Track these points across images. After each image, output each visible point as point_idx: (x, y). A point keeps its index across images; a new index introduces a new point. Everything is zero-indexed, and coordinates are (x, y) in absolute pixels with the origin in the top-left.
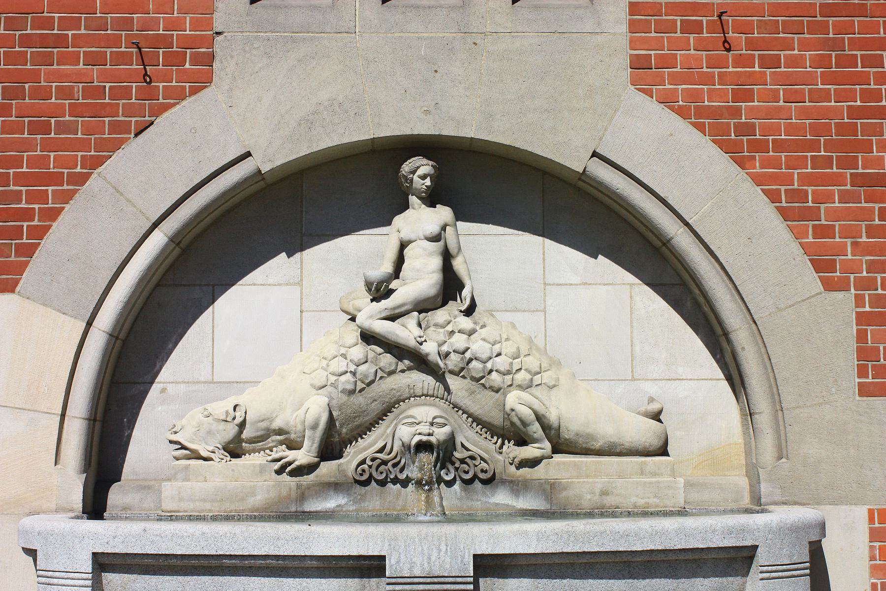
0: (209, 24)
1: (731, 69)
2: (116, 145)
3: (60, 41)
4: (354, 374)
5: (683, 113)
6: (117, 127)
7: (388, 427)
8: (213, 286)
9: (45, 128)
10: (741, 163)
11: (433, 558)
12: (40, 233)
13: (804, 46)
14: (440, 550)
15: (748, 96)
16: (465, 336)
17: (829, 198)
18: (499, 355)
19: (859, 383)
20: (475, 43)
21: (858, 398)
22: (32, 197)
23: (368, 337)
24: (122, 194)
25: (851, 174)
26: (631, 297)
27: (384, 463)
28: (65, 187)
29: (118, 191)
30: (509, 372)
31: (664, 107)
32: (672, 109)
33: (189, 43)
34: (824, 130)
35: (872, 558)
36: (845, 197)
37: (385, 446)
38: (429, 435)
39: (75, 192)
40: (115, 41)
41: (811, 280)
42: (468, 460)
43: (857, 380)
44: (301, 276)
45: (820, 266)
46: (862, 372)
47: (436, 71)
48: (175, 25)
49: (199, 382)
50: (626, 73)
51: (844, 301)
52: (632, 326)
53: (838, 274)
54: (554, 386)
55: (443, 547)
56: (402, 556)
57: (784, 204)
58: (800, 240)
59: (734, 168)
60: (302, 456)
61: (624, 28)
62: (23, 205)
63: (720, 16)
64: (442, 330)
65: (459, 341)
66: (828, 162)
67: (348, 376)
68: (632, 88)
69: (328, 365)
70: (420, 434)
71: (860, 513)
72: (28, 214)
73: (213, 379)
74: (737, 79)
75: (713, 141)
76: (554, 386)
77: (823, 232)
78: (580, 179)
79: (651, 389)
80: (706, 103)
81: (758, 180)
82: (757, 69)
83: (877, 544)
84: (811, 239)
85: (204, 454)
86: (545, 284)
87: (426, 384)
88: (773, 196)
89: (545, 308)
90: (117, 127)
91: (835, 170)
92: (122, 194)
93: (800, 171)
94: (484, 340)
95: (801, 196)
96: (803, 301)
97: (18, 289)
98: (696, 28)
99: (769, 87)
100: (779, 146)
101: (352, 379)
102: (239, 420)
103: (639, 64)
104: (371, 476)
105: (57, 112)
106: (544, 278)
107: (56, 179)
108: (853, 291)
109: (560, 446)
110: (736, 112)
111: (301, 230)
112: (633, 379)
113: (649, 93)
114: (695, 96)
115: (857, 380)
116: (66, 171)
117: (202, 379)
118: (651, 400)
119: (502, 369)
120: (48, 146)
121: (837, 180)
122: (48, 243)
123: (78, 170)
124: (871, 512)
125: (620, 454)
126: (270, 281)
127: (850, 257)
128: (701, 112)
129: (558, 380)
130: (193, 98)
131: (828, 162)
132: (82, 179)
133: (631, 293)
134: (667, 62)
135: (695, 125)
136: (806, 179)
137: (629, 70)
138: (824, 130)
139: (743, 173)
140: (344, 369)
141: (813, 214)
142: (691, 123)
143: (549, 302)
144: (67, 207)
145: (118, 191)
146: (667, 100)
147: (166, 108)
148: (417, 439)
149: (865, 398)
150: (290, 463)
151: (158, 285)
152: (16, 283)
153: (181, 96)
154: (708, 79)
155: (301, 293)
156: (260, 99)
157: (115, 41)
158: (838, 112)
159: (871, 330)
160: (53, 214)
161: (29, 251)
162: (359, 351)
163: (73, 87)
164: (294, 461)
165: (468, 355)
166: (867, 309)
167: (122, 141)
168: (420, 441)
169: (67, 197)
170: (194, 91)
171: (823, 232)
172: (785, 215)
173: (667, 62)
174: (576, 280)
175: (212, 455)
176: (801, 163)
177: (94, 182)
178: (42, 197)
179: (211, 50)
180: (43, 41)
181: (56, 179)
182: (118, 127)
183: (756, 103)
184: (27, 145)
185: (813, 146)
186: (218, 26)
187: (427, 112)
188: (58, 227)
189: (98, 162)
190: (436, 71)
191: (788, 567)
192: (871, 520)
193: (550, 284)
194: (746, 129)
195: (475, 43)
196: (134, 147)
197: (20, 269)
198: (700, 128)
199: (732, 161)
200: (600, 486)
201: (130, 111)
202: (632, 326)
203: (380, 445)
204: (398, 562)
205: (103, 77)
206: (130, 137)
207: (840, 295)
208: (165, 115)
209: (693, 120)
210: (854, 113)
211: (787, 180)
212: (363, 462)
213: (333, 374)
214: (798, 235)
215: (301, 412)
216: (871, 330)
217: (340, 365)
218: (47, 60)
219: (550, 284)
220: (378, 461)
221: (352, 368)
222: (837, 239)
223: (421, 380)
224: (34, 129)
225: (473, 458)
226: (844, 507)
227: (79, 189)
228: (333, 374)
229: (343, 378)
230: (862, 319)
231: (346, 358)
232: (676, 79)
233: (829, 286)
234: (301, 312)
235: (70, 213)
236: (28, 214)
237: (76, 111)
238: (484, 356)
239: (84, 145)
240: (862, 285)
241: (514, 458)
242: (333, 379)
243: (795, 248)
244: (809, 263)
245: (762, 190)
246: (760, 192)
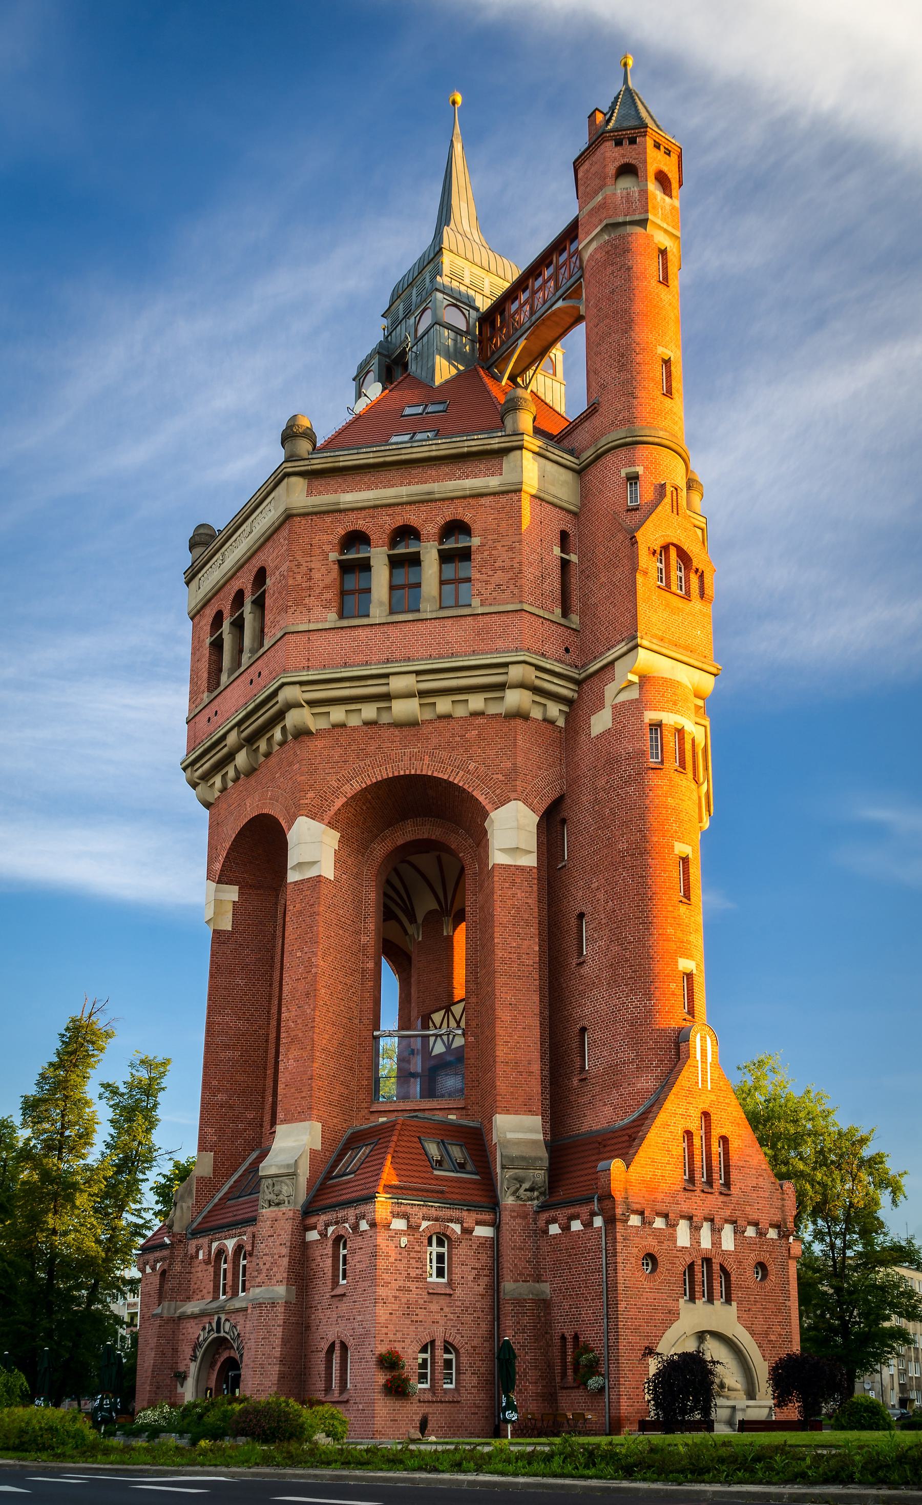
0: (678, 1307)
2: (666, 1330)
6: (666, 1327)
22: (656, 1340)
33: (676, 1310)
41: (762, 1358)
45: (763, 1357)
48: (674, 1307)
51: (767, 1362)
103: (738, 1317)
107: (658, 1336)
132: (662, 1337)
141: (762, 1347)
146: (742, 1324)
153: (675, 1321)
160: (658, 1343)
171: (764, 1350)
173: (742, 1317)
181: (658, 1336)
189: (663, 1333)
194: (753, 1330)
233: (765, 1360)
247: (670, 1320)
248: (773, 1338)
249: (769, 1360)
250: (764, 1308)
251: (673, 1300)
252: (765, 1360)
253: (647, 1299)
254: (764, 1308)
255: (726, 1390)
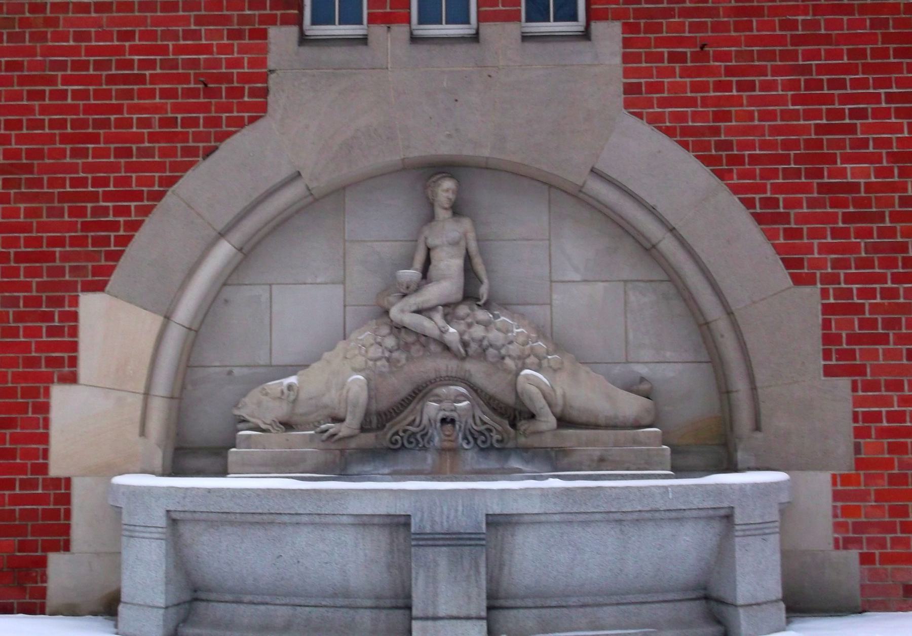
0: (263, 63)
1: (712, 94)
2: (186, 167)
3: (141, 79)
4: (388, 360)
5: (669, 132)
6: (188, 152)
7: (418, 403)
8: (270, 285)
9: (128, 153)
10: (721, 175)
11: (452, 517)
12: (125, 241)
13: (776, 71)
14: (456, 511)
15: (726, 116)
16: (482, 328)
17: (798, 204)
18: (511, 342)
19: (825, 365)
20: (490, 76)
21: (823, 378)
22: (119, 211)
23: (398, 328)
24: (192, 208)
25: (818, 184)
26: (625, 292)
27: (414, 434)
28: (146, 203)
29: (189, 206)
30: (519, 358)
31: (654, 128)
32: (660, 129)
34: (795, 145)
35: (835, 516)
36: (812, 203)
37: (414, 420)
38: (452, 410)
39: (153, 207)
40: (185, 79)
41: (783, 276)
42: (486, 433)
43: (823, 363)
44: (345, 277)
45: (789, 264)
46: (827, 355)
47: (456, 100)
49: (259, 366)
50: (620, 100)
52: (626, 317)
53: (806, 271)
54: (559, 369)
55: (460, 508)
56: (425, 515)
57: (758, 210)
58: (772, 242)
59: (715, 180)
60: (343, 430)
61: (618, 60)
62: (111, 218)
63: (702, 47)
64: (462, 322)
65: (478, 331)
66: (797, 173)
67: (384, 362)
68: (625, 112)
69: (366, 352)
70: (444, 410)
71: (825, 477)
72: (114, 226)
73: (271, 362)
74: (718, 101)
75: (698, 157)
76: (559, 369)
77: (792, 234)
78: (580, 191)
79: (642, 370)
80: (690, 124)
81: (735, 190)
82: (735, 93)
83: (839, 504)
84: (782, 241)
85: (263, 426)
86: (551, 281)
87: (450, 367)
88: (748, 204)
89: (551, 300)
90: (188, 152)
91: (803, 180)
92: (192, 208)
93: (772, 181)
94: (498, 330)
95: (774, 203)
96: (775, 294)
97: (108, 288)
98: (681, 58)
99: (745, 108)
100: (754, 159)
101: (387, 364)
102: (292, 398)
103: (629, 89)
104: (403, 445)
105: (139, 138)
106: (550, 277)
108: (819, 286)
109: (564, 422)
110: (716, 131)
111: (344, 236)
112: (627, 362)
113: (639, 116)
114: (681, 117)
115: (823, 363)
116: (145, 189)
117: (262, 363)
118: (642, 379)
119: (514, 354)
120: (131, 167)
121: (805, 188)
122: (131, 250)
123: (156, 188)
124: (834, 477)
125: (615, 427)
126: (319, 280)
127: (816, 256)
128: (686, 131)
129: (562, 363)
130: (251, 126)
131: (797, 173)
132: (158, 196)
133: (625, 288)
134: (656, 88)
135: (679, 142)
136: (777, 188)
137: (623, 96)
138: (795, 145)
139: (722, 183)
140: (380, 355)
141: (785, 218)
142: (677, 141)
143: (555, 296)
144: (147, 219)
145: (189, 206)
146: (654, 120)
147: (229, 134)
148: (441, 415)
149: (829, 378)
150: (333, 435)
151: (225, 284)
152: (105, 283)
153: (240, 124)
154: (692, 102)
155: (345, 291)
156: (307, 127)
157: (185, 79)
158: (805, 130)
159: (836, 320)
160: (135, 226)
161: (115, 256)
162: (390, 342)
163: (150, 118)
164: (340, 431)
165: (485, 343)
166: (832, 301)
167: (191, 165)
168: (444, 415)
169: (146, 211)
170: (252, 120)
171: (792, 234)
172: (759, 219)
173: (656, 88)
174: (578, 277)
175: (270, 427)
176: (774, 174)
177: (170, 198)
178: (126, 211)
179: (265, 85)
180: (126, 79)
181: (138, 196)
182: (191, 152)
183: (734, 123)
184: (114, 168)
185: (785, 159)
186: (271, 65)
187: (449, 136)
188: (140, 237)
190: (456, 100)
191: (761, 526)
192: (834, 483)
193: (555, 282)
194: (727, 145)
195: (490, 76)
196: (203, 169)
197: (109, 271)
198: (685, 145)
199: (712, 173)
200: (598, 453)
201: (198, 137)
202: (626, 317)
203: (411, 418)
204: (421, 520)
205: (177, 108)
206: (198, 161)
207: (807, 290)
208: (228, 141)
209: (678, 138)
210: (820, 129)
211: (761, 189)
212: (397, 433)
213: (371, 360)
214: (771, 236)
215: (345, 391)
216: (836, 320)
217: (375, 352)
218: (128, 94)
219: (555, 282)
220: (409, 433)
221: (387, 354)
222: (805, 241)
223: (445, 365)
224: (120, 153)
225: (489, 430)
226: (812, 473)
227: (156, 205)
228: (371, 360)
229: (379, 363)
230: (827, 309)
231: (381, 346)
232: (663, 103)
233: (798, 280)
234: (345, 306)
235: (150, 224)
236: (114, 226)
237: (153, 137)
238: (499, 343)
239: (160, 167)
240: (827, 279)
241: (525, 430)
242: (371, 363)
243: (768, 249)
244: (780, 262)
245: (740, 199)
246: (737, 200)
247: (214, 122)
248: (851, 172)
249: (834, 279)
250: (798, 40)
251: (235, 35)
252: (798, 280)
253: (81, 36)
254: (798, 40)
255: (548, 421)
